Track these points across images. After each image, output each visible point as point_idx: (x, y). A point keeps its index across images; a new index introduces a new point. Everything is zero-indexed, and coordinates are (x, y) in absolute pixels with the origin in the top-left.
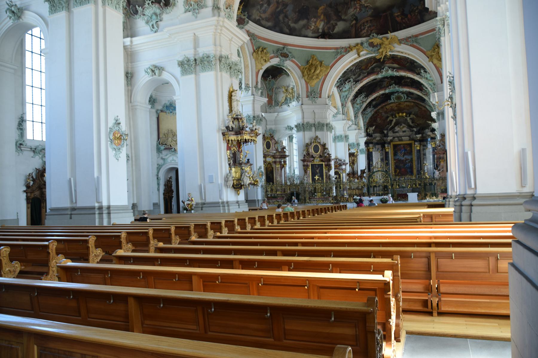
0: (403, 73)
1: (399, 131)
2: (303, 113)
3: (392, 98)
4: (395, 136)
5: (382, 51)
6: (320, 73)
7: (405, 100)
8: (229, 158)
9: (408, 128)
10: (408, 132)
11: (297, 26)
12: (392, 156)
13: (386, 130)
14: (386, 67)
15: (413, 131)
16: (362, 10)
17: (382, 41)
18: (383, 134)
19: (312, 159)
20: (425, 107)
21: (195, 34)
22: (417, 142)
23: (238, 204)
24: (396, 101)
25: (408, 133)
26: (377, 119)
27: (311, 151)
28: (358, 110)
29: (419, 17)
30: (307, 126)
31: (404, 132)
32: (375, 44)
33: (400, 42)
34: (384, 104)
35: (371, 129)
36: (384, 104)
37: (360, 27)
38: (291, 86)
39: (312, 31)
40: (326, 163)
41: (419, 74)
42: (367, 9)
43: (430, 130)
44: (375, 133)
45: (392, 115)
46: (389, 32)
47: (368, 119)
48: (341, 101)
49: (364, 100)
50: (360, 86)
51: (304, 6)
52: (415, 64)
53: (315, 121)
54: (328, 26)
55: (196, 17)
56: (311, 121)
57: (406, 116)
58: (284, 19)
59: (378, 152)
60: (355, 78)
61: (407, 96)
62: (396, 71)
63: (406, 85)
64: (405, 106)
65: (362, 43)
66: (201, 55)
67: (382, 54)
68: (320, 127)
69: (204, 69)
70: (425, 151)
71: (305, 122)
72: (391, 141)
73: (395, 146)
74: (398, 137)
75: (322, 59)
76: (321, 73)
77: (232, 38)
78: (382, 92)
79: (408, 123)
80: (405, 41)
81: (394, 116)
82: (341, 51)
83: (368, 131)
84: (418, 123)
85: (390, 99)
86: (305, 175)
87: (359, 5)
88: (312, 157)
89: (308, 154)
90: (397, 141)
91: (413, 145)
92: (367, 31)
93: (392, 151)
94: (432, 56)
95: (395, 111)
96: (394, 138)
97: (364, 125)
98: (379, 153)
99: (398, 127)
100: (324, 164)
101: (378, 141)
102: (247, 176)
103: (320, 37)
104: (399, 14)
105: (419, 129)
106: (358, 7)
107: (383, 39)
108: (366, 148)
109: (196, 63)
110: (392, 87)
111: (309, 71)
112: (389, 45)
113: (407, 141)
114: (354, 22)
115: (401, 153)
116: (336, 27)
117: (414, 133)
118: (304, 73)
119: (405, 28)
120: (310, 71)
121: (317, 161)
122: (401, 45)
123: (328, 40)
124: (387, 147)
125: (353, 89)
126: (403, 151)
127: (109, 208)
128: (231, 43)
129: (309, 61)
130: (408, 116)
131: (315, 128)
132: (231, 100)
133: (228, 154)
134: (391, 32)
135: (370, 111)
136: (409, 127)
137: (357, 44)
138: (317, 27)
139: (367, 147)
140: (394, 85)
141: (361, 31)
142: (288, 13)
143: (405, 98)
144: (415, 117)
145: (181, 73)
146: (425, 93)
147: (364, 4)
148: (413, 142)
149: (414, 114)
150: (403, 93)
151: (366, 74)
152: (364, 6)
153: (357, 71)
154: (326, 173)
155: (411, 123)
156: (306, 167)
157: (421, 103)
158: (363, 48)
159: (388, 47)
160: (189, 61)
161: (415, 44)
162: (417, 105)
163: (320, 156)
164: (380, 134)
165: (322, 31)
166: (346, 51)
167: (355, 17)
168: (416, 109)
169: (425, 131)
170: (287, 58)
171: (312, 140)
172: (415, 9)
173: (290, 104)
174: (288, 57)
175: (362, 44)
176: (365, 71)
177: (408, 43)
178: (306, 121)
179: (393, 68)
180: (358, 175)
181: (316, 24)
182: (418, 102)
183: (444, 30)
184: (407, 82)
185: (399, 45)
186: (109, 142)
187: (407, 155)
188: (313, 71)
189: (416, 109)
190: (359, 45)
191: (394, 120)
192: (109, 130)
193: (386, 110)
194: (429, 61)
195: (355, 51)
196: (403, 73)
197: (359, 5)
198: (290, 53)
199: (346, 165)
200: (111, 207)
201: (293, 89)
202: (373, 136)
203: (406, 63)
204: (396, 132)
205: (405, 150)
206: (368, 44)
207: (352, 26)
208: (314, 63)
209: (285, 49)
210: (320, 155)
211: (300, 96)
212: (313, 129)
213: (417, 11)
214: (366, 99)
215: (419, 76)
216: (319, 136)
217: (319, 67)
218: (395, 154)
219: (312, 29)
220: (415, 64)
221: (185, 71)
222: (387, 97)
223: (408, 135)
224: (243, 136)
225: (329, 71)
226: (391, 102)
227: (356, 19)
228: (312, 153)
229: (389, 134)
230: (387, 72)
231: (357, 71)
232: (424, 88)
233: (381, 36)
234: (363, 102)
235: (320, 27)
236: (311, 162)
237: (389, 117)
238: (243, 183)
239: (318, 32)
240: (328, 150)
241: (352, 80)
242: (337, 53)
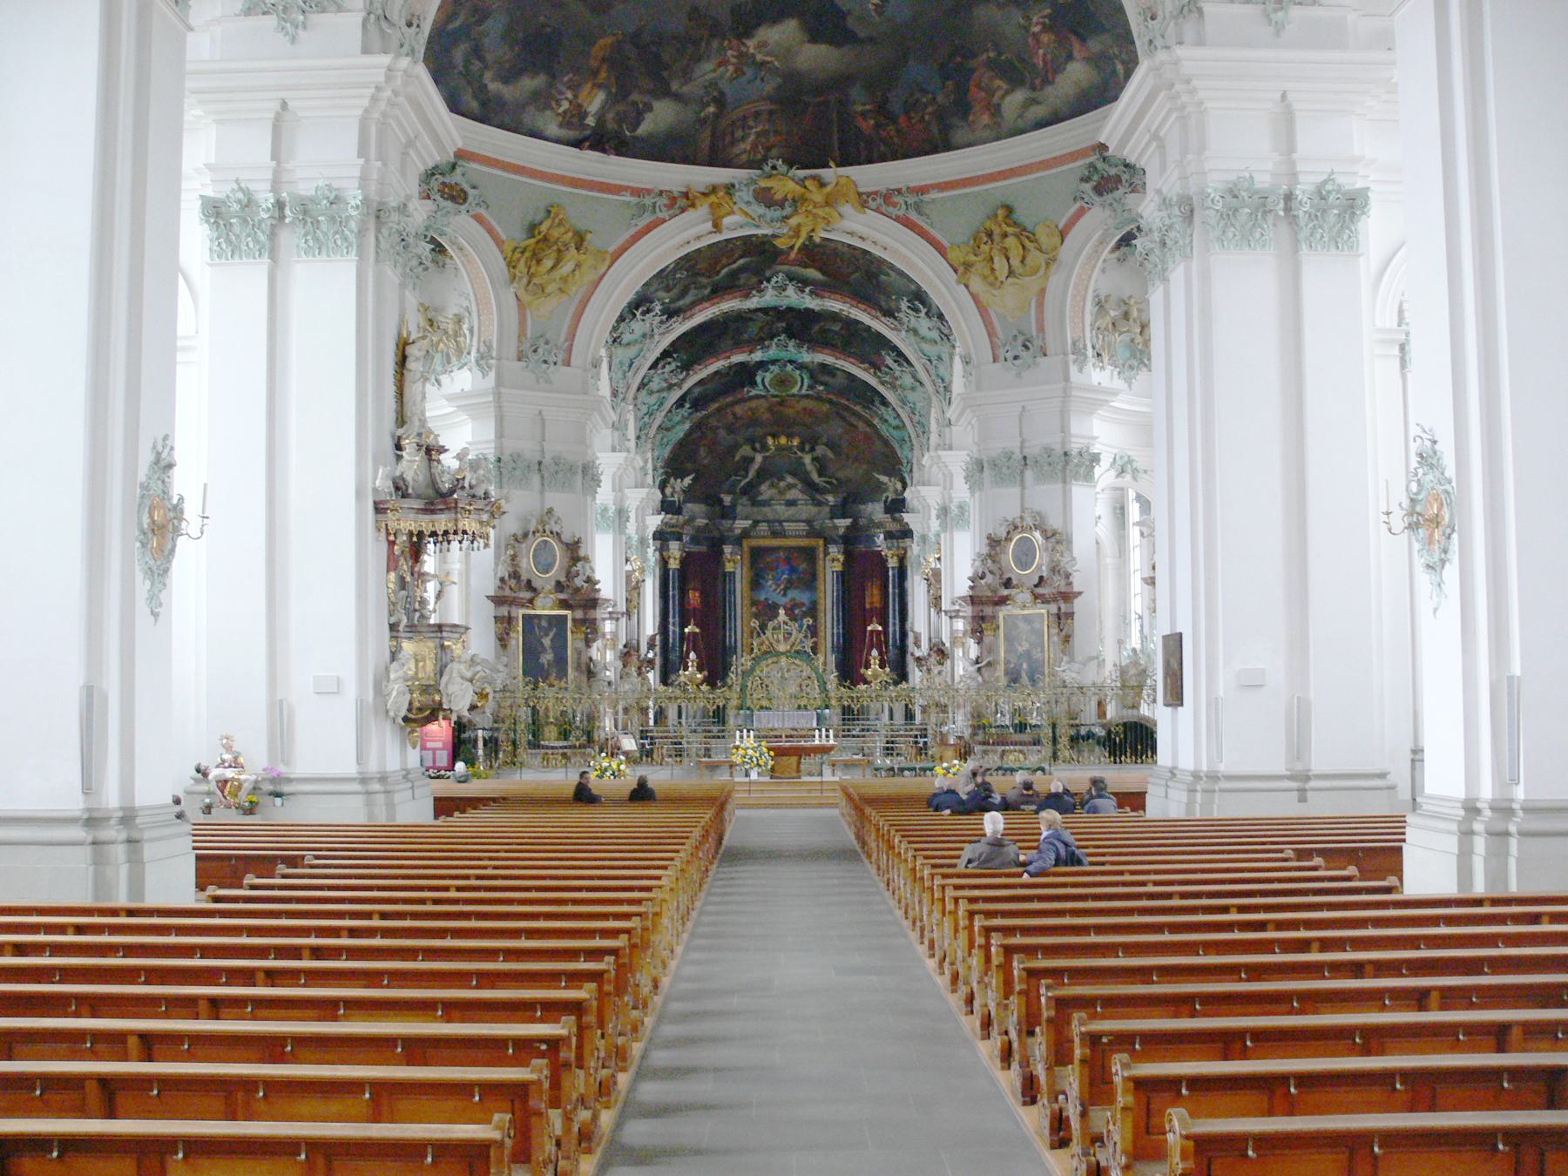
0: (834, 305)
1: (772, 499)
2: (500, 421)
3: (758, 379)
4: (760, 518)
5: (799, 225)
6: (574, 275)
7: (804, 392)
8: (394, 604)
9: (802, 492)
10: (806, 504)
11: (509, 92)
12: (745, 589)
13: (729, 492)
14: (781, 275)
15: (819, 504)
16: (744, 74)
17: (803, 190)
18: (717, 508)
19: (527, 595)
20: (869, 423)
21: (284, 105)
22: (834, 542)
23: (410, 785)
24: (772, 391)
25: (806, 510)
27: (527, 565)
28: (650, 414)
29: (935, 130)
30: (514, 469)
31: (791, 503)
32: (778, 197)
33: (864, 200)
34: (729, 399)
35: (680, 485)
36: (729, 399)
37: (730, 130)
38: (452, 310)
39: (561, 119)
40: (579, 614)
41: (889, 313)
42: (763, 73)
43: (882, 505)
45: (751, 441)
46: (832, 164)
47: (669, 448)
48: (611, 379)
49: (675, 381)
50: (681, 327)
51: (544, 26)
52: (883, 277)
53: (543, 451)
54: (620, 108)
55: (293, 40)
56: (529, 450)
57: (802, 449)
58: (467, 62)
60: (670, 303)
61: (812, 377)
62: (811, 292)
63: (821, 342)
65: (733, 186)
66: (306, 189)
67: (797, 235)
68: (560, 475)
69: (319, 246)
71: (507, 452)
72: (746, 534)
73: (757, 554)
74: (768, 521)
75: (581, 225)
76: (577, 272)
77: (416, 137)
78: (738, 358)
79: (807, 473)
80: (880, 201)
81: (758, 446)
82: (655, 203)
83: (668, 491)
84: (840, 474)
85: (753, 384)
86: (497, 657)
87: (735, 53)
88: (529, 586)
89: (515, 575)
90: (764, 537)
91: (821, 556)
92: (754, 146)
93: (745, 569)
94: (968, 266)
96: (756, 523)
97: (655, 469)
99: (772, 485)
100: (570, 618)
101: (699, 529)
102: (462, 678)
103: (587, 144)
104: (868, 107)
105: (845, 502)
106: (733, 60)
107: (807, 183)
108: (657, 553)
109: (282, 217)
110: (777, 345)
111: (534, 262)
112: (827, 209)
113: (801, 537)
114: (711, 109)
115: (777, 580)
116: (649, 117)
117: (827, 509)
118: (514, 267)
119: (883, 159)
120: (539, 262)
121: (545, 608)
122: (865, 213)
123: (614, 159)
125: (656, 337)
126: (783, 573)
127: (128, 818)
128: (405, 154)
129: (540, 224)
130: (807, 447)
131: (542, 477)
132: (402, 374)
133: (391, 585)
134: (839, 165)
135: (677, 419)
136: (810, 486)
137: (714, 189)
138: (580, 106)
139: (661, 555)
140: (783, 337)
141: (733, 143)
142: (487, 41)
143: (805, 387)
144: (830, 454)
145: (211, 250)
146: (887, 378)
147: (753, 55)
148: (821, 542)
149: (826, 445)
150: (801, 367)
151: (706, 292)
152: (754, 62)
153: (678, 276)
154: (579, 653)
155: (815, 476)
156: (505, 625)
157: (858, 408)
158: (735, 203)
159: (819, 212)
160: (249, 203)
161: (913, 216)
162: (840, 413)
163: (559, 587)
165: (597, 123)
166: (670, 206)
167: (715, 94)
168: (836, 429)
169: (863, 507)
170: (461, 204)
171: (529, 521)
172: (924, 100)
173: (444, 379)
174: (465, 200)
175: (730, 188)
176: (704, 280)
177: (890, 209)
178: (511, 445)
179: (803, 283)
180: (639, 656)
181: (576, 96)
182: (846, 403)
183: (1191, 235)
184: (829, 330)
185: (860, 212)
186: (138, 544)
187: (795, 588)
188: (548, 263)
189: (836, 429)
190: (721, 194)
191: (759, 458)
192: (139, 491)
194: (958, 282)
195: (703, 210)
196: (834, 305)
197: (735, 53)
198: (474, 188)
199: (617, 619)
200: (140, 813)
201: (459, 320)
202: (685, 510)
203: (850, 270)
204: (766, 503)
205: (792, 570)
206: (751, 192)
207: (703, 122)
208: (555, 233)
209: (459, 170)
210: (558, 583)
211: (494, 355)
212: (536, 478)
213: (930, 109)
214: (681, 377)
215: (892, 320)
216: (558, 512)
217: (573, 251)
218: (756, 584)
219: (561, 110)
220: (883, 277)
221: (229, 241)
222: (745, 374)
223: (804, 518)
224: (456, 520)
225: (603, 270)
226: (753, 393)
227: (720, 101)
228: (529, 571)
229: (739, 508)
230: (777, 294)
231: (678, 276)
232: (889, 361)
233: (802, 173)
234: (670, 387)
235: (588, 110)
236: (523, 606)
238: (450, 702)
239: (584, 126)
240: (587, 566)
241: (658, 308)
242: (642, 209)
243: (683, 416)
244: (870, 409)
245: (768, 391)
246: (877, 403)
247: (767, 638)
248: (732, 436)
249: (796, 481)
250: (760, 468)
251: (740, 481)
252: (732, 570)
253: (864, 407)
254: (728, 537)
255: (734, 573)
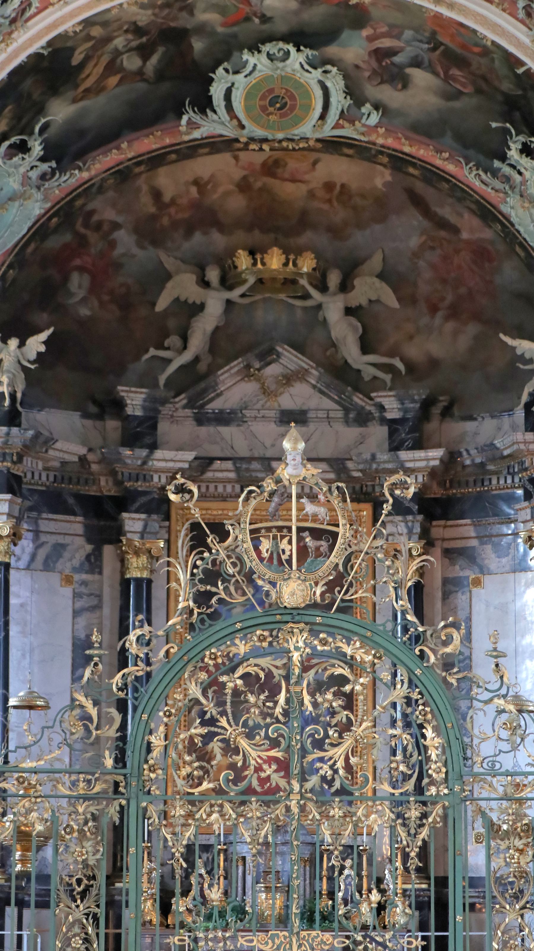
4: (214, 451)
26: (66, 279)
43: (520, 414)
44: (42, 408)
59: (55, 578)
64: (311, 194)
70: (461, 599)
95: (221, 228)
98: (68, 591)
124: (142, 535)
149: (381, 276)
164: (86, 415)
169: (470, 426)
193: (152, 210)
229: (163, 427)
237: (169, 276)
243: (26, 180)
244: (495, 173)
245: (243, 127)
246: (513, 153)
247: (231, 551)
248: (151, 252)
249: (303, 362)
250: (217, 329)
251: (169, 361)
252: (145, 575)
253: (478, 166)
254: (136, 494)
255: (149, 582)
